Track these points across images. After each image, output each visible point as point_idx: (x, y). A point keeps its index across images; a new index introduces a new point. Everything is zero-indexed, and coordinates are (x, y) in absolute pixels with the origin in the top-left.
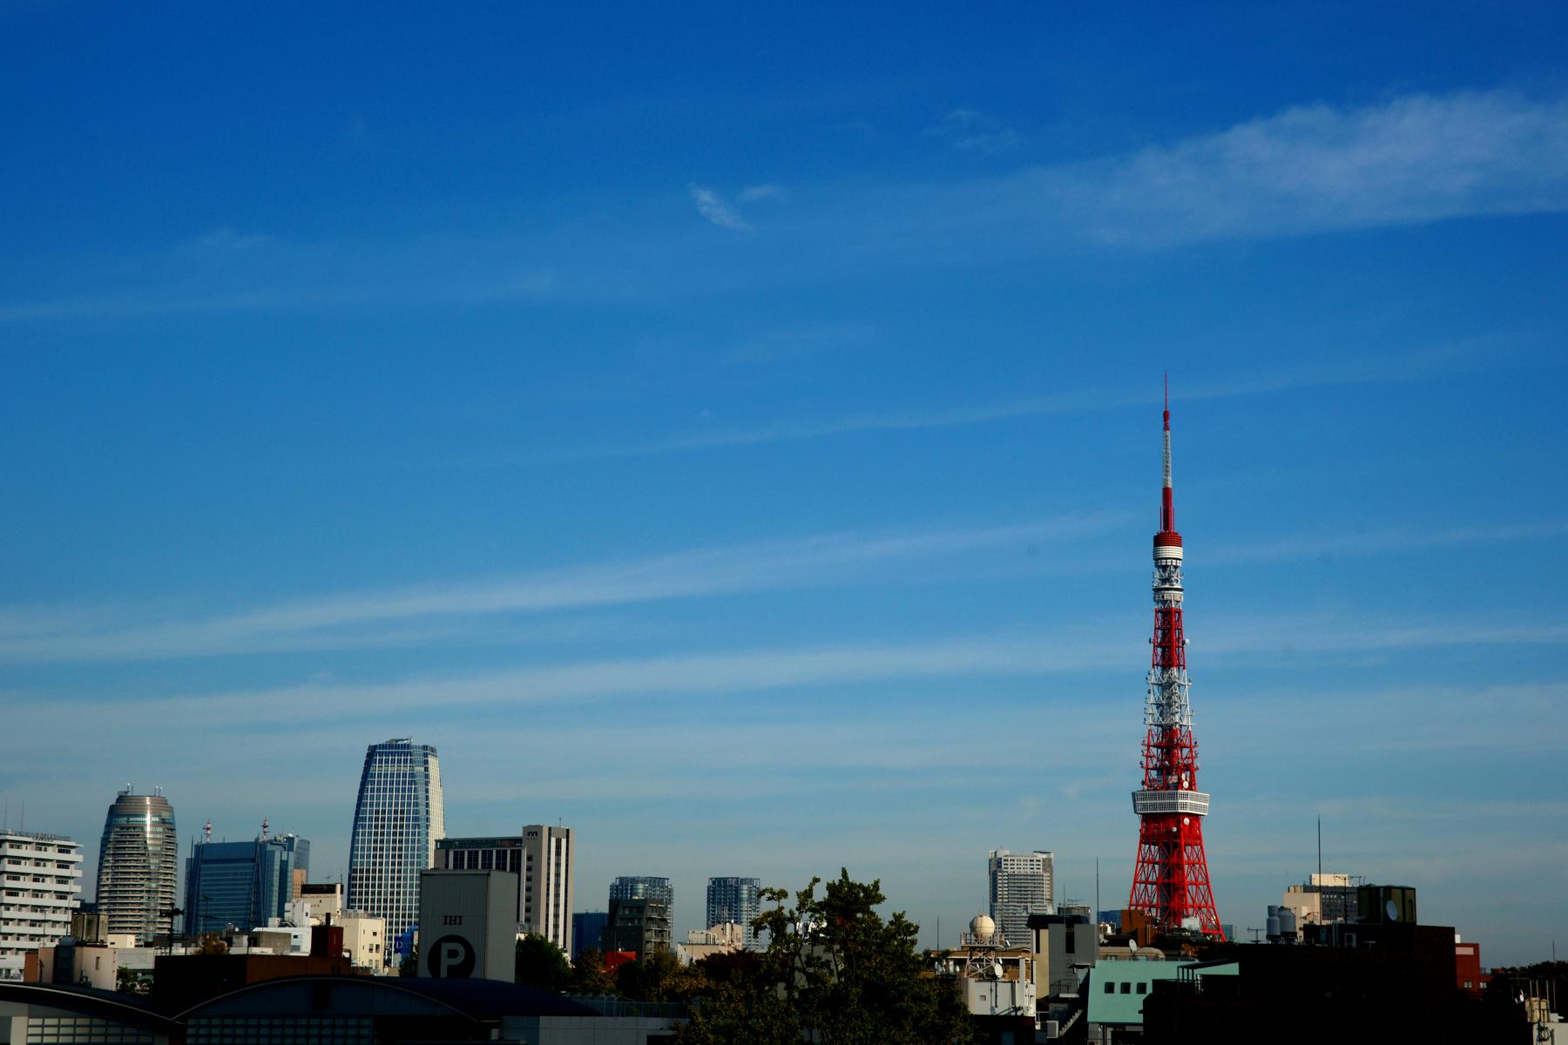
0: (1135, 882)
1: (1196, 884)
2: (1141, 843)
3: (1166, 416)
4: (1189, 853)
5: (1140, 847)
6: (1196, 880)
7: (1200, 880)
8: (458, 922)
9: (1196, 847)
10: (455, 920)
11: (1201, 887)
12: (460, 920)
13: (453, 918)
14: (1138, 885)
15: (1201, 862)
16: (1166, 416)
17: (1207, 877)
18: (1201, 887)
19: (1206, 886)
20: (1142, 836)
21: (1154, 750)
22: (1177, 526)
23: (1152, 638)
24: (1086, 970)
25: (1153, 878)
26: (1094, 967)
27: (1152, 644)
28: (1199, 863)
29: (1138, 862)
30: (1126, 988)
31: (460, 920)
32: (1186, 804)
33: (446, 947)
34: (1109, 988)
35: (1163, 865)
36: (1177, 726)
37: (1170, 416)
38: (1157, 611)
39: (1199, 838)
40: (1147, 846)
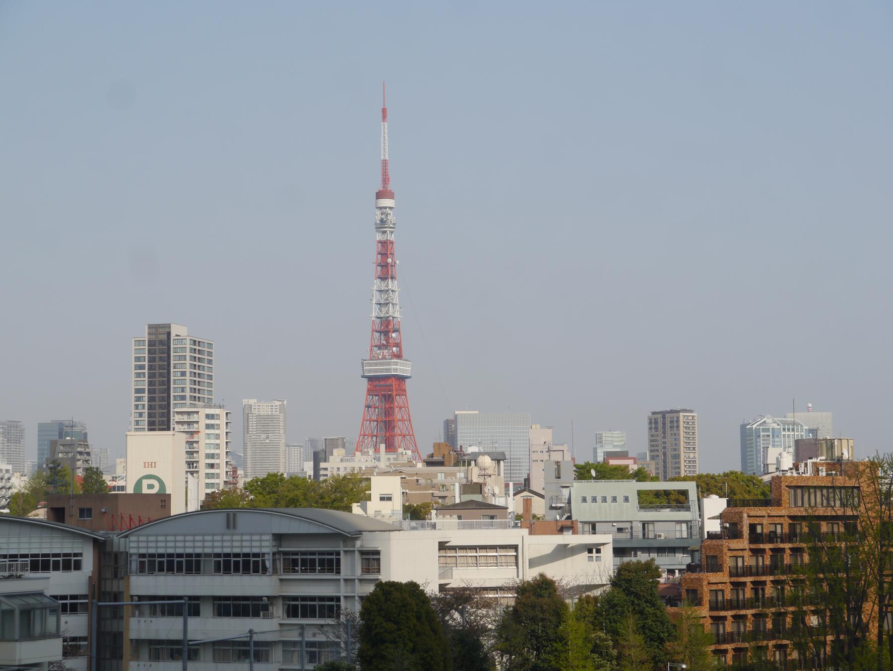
0: (364, 420)
1: (402, 420)
3: (384, 111)
4: (398, 400)
7: (405, 418)
8: (147, 464)
9: (402, 397)
10: (152, 465)
11: (406, 422)
12: (145, 465)
13: (150, 464)
14: (365, 422)
16: (384, 111)
17: (409, 415)
18: (406, 422)
19: (409, 422)
20: (368, 390)
21: (377, 335)
22: (391, 187)
24: (568, 489)
25: (374, 417)
26: (573, 487)
30: (604, 500)
31: (145, 465)
32: (397, 369)
33: (145, 483)
34: (584, 500)
36: (391, 318)
37: (388, 112)
39: (405, 391)
40: (371, 396)
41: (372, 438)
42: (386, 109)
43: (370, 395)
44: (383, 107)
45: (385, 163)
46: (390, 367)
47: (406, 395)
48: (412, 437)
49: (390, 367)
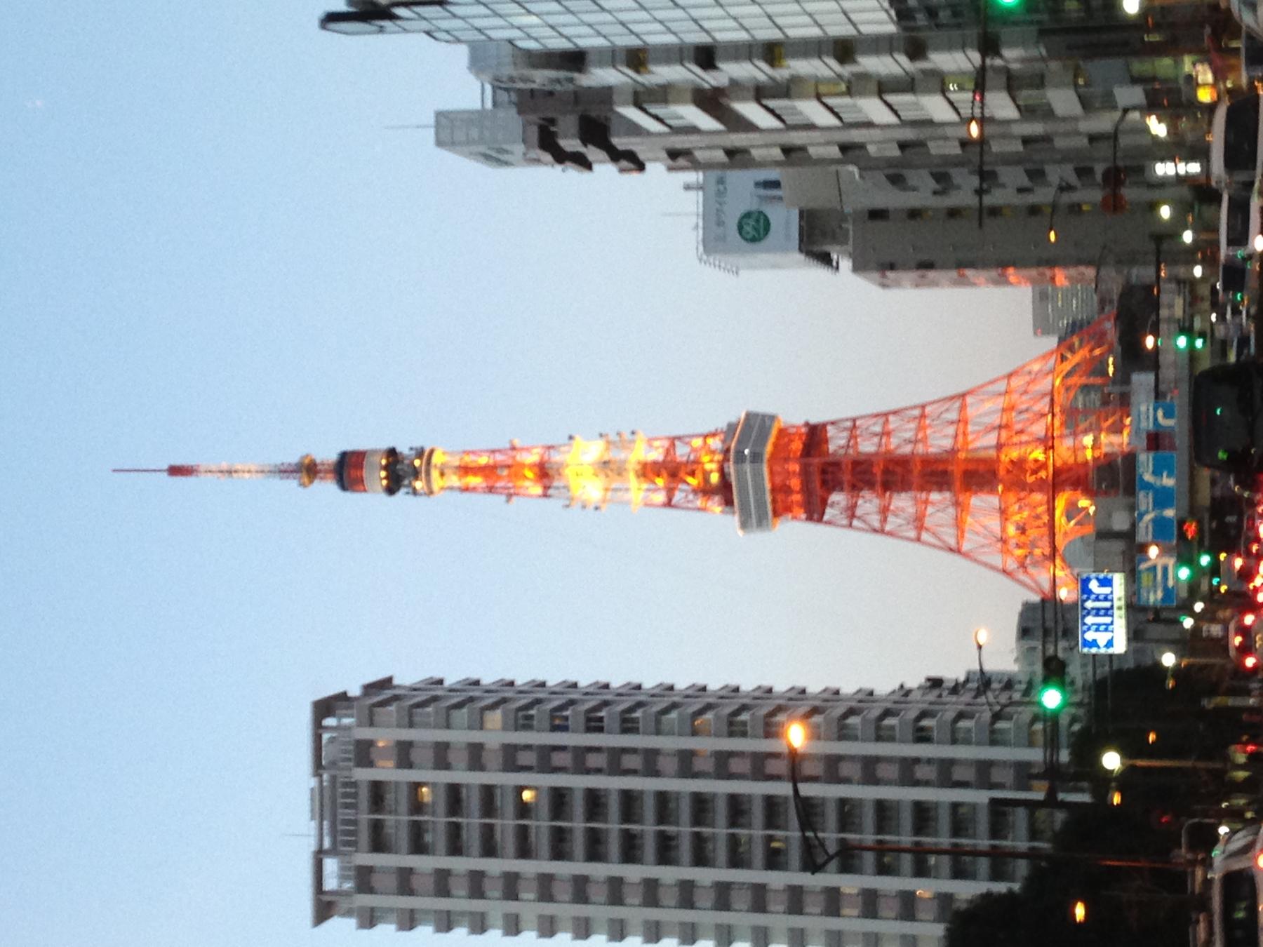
0: (881, 531)
1: (886, 433)
2: (820, 520)
3: (175, 471)
5: (829, 523)
6: (876, 435)
7: (878, 429)
11: (891, 426)
14: (888, 528)
15: (853, 428)
16: (175, 471)
19: (891, 418)
20: (810, 518)
23: (503, 498)
35: (855, 488)
37: (178, 462)
41: (933, 503)
43: (823, 513)
44: (165, 474)
48: (928, 409)
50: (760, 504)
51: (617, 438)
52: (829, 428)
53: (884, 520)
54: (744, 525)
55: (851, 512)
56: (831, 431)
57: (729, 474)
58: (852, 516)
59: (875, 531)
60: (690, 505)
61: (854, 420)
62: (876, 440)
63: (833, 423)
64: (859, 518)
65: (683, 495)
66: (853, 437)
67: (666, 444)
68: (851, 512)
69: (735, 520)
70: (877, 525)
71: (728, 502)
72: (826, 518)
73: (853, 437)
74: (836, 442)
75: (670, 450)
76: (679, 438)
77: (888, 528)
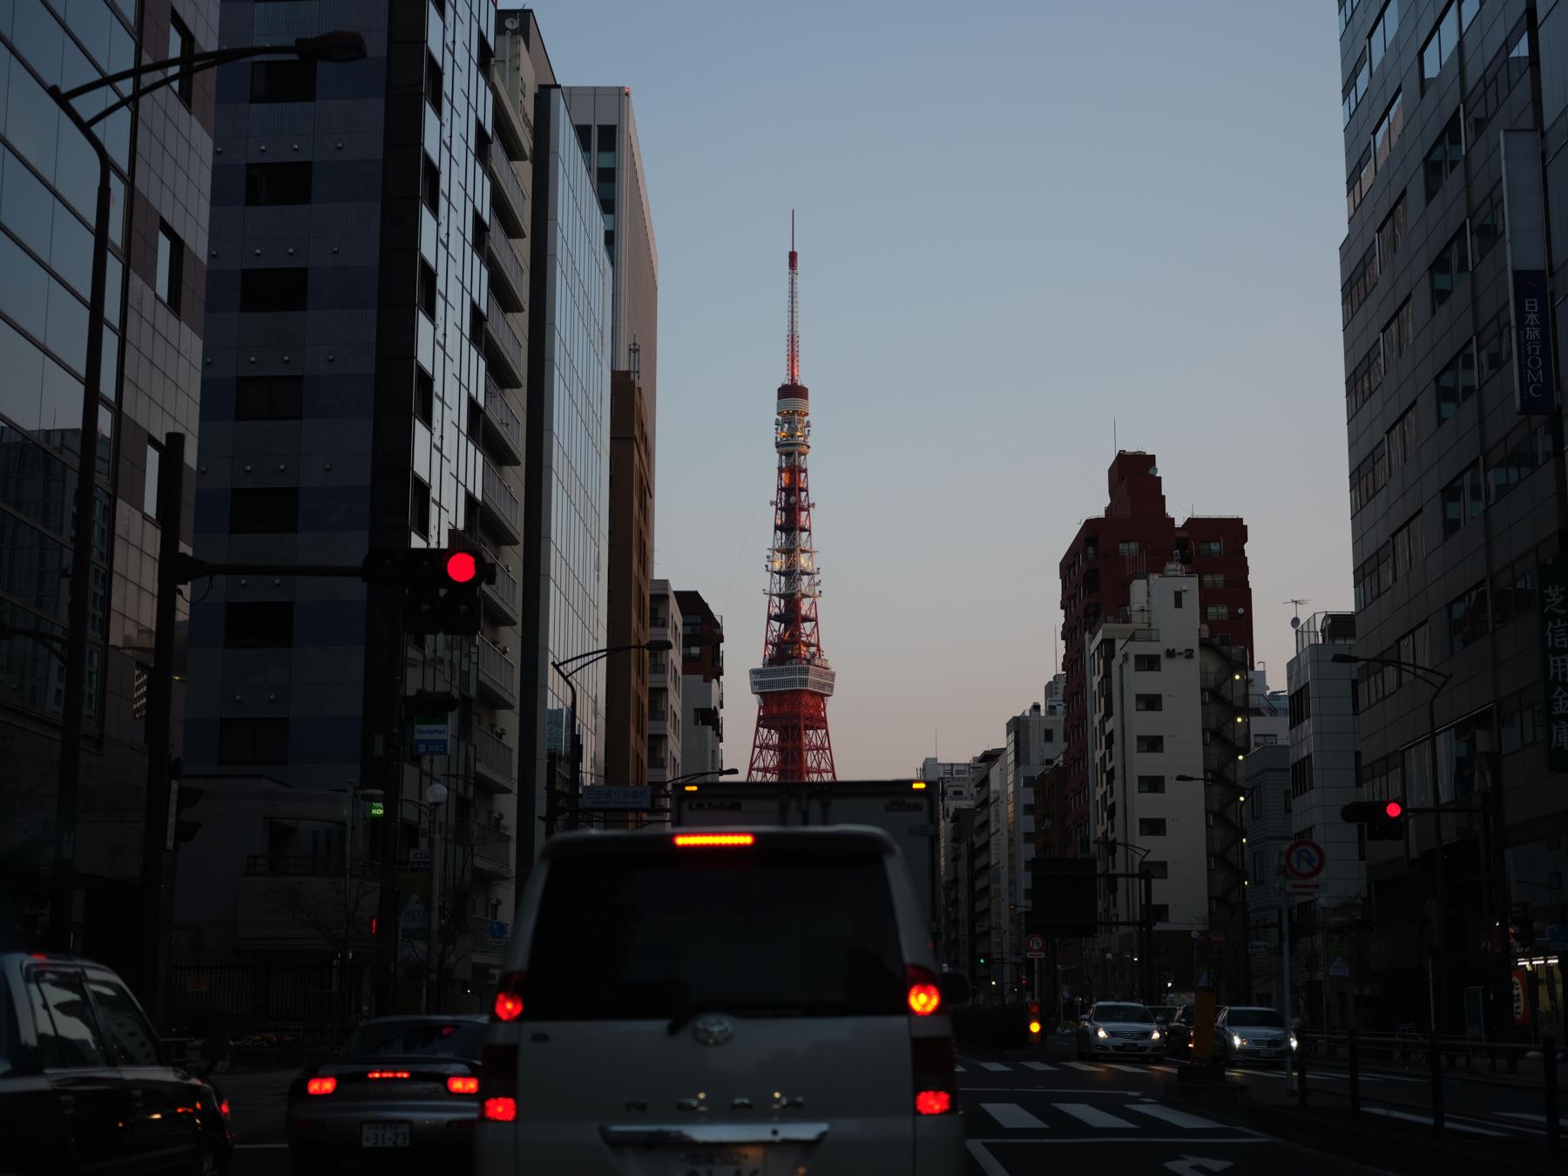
2: (758, 725)
3: (793, 256)
4: (813, 737)
6: (819, 764)
7: (823, 766)
9: (819, 731)
14: (754, 773)
16: (793, 256)
17: (832, 765)
19: (831, 774)
23: (774, 499)
27: (774, 507)
28: (824, 749)
29: (755, 746)
35: (780, 748)
37: (799, 259)
38: (780, 470)
39: (824, 720)
40: (766, 730)
42: (796, 253)
43: (764, 727)
45: (793, 340)
46: (795, 677)
47: (826, 728)
49: (795, 677)
50: (771, 684)
51: (816, 581)
52: (824, 731)
53: (758, 770)
54: (754, 672)
55: (764, 747)
56: (821, 732)
57: (791, 664)
58: (761, 747)
59: (752, 764)
60: (769, 633)
61: (829, 749)
62: (815, 765)
63: (827, 733)
64: (761, 752)
65: (777, 629)
66: (818, 749)
67: (813, 615)
68: (764, 747)
69: (759, 665)
70: (756, 765)
71: (771, 661)
72: (761, 729)
73: (818, 749)
74: (813, 737)
75: (806, 619)
76: (816, 625)
77: (754, 773)
